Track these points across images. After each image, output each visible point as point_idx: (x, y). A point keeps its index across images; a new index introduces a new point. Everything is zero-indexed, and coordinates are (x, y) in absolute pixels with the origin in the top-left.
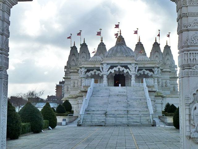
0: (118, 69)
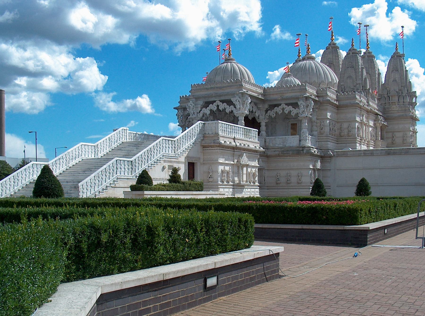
0: (216, 108)
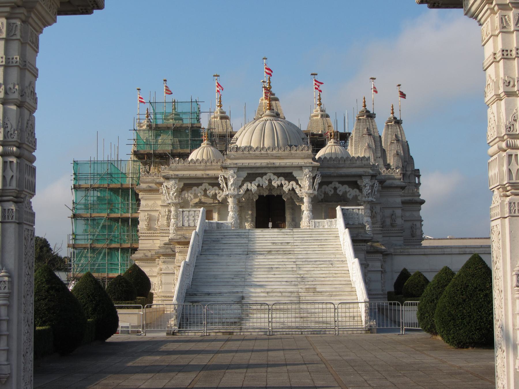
0: (267, 182)
